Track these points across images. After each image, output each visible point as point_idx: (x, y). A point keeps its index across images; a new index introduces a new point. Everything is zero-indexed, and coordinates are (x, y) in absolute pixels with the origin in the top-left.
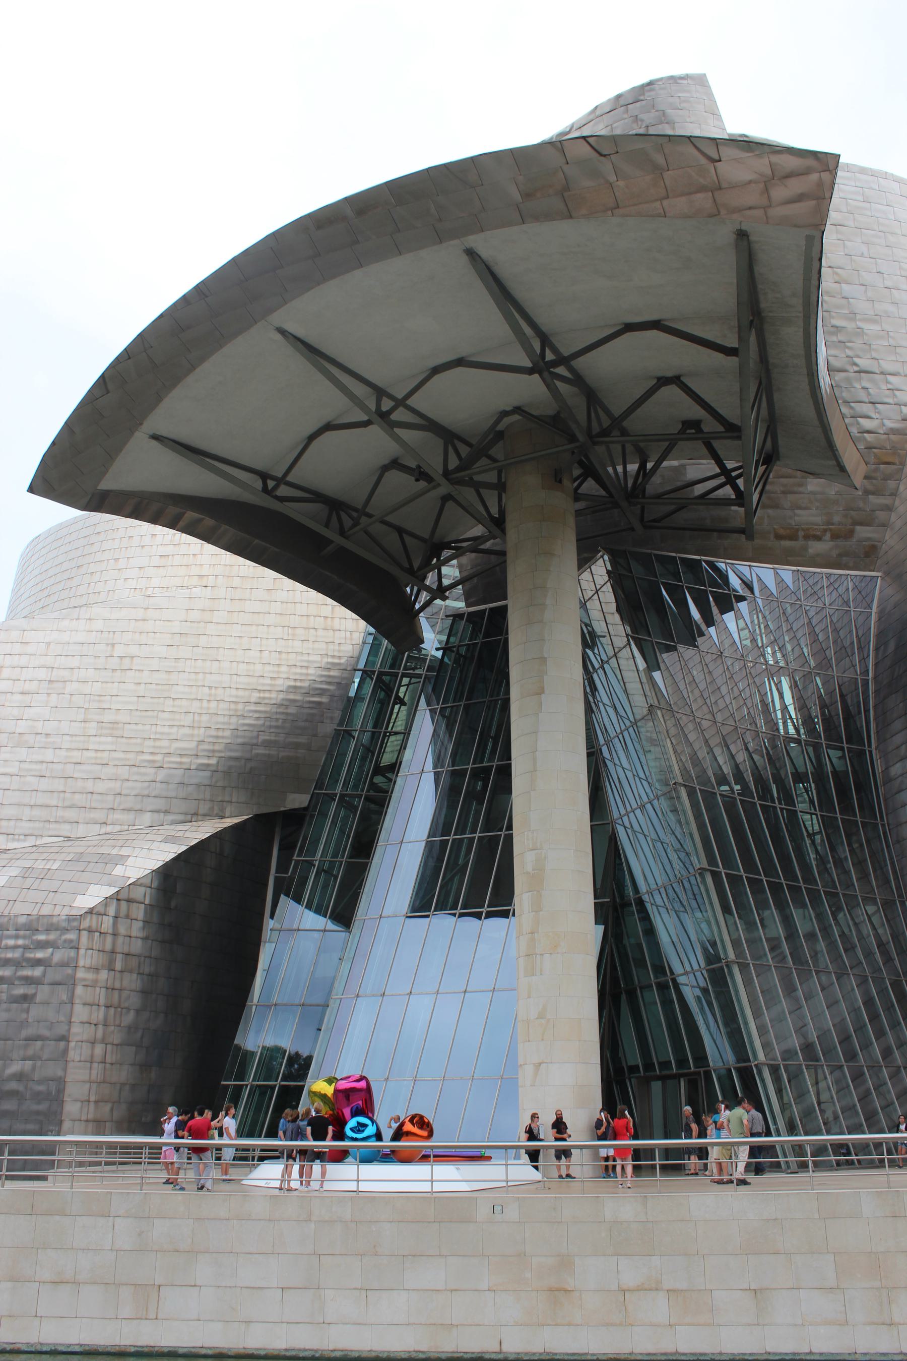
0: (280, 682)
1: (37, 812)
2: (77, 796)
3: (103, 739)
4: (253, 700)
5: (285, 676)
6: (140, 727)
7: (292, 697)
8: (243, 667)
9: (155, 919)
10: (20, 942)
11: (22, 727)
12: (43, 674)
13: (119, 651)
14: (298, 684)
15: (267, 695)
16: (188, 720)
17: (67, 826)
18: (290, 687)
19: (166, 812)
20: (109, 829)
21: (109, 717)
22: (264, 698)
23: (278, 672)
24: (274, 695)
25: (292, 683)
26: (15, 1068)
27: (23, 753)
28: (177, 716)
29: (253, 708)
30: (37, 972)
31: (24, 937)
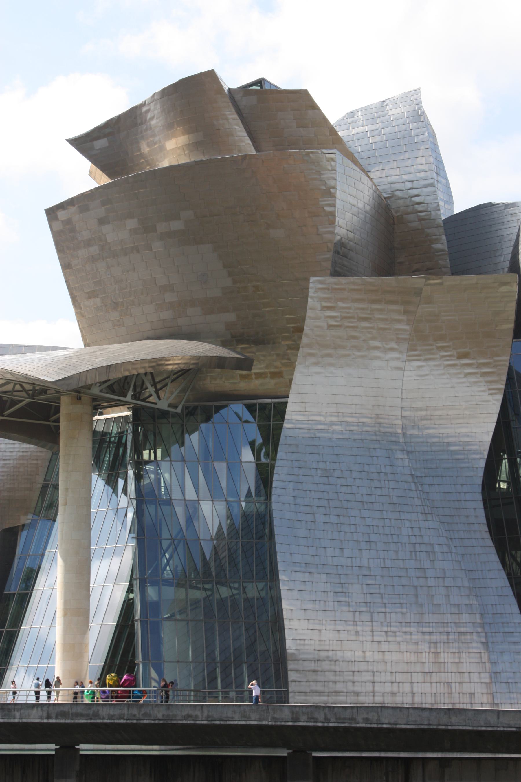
0: (14, 454)
5: (17, 450)
7: (21, 462)
14: (25, 454)
15: (8, 462)
18: (20, 456)
22: (6, 464)
23: (14, 448)
24: (11, 462)
25: (21, 454)
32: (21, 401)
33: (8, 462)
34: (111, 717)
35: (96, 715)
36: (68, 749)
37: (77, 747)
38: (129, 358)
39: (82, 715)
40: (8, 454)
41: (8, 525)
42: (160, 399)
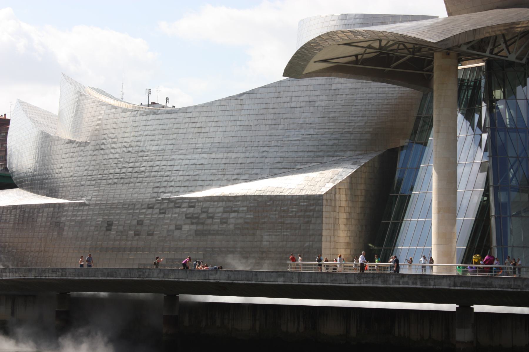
0: (395, 95)
1: (310, 154)
2: (323, 147)
3: (331, 124)
4: (385, 103)
5: (397, 92)
6: (343, 118)
8: (381, 90)
9: (349, 193)
10: (305, 204)
11: (301, 121)
12: (307, 99)
13: (334, 87)
14: (402, 95)
15: (390, 101)
16: (361, 114)
17: (320, 159)
18: (399, 96)
19: (355, 151)
20: (335, 158)
21: (332, 115)
22: (389, 102)
23: (395, 91)
24: (393, 101)
25: (400, 95)
26: (307, 244)
27: (303, 131)
28: (357, 113)
29: (385, 107)
30: (311, 213)
31: (306, 202)
32: (404, 57)
33: (390, 101)
34: (501, 287)
35: (490, 285)
36: (465, 308)
37: (472, 306)
38: (489, 23)
39: (479, 285)
40: (390, 95)
41: (392, 146)
42: (510, 54)
